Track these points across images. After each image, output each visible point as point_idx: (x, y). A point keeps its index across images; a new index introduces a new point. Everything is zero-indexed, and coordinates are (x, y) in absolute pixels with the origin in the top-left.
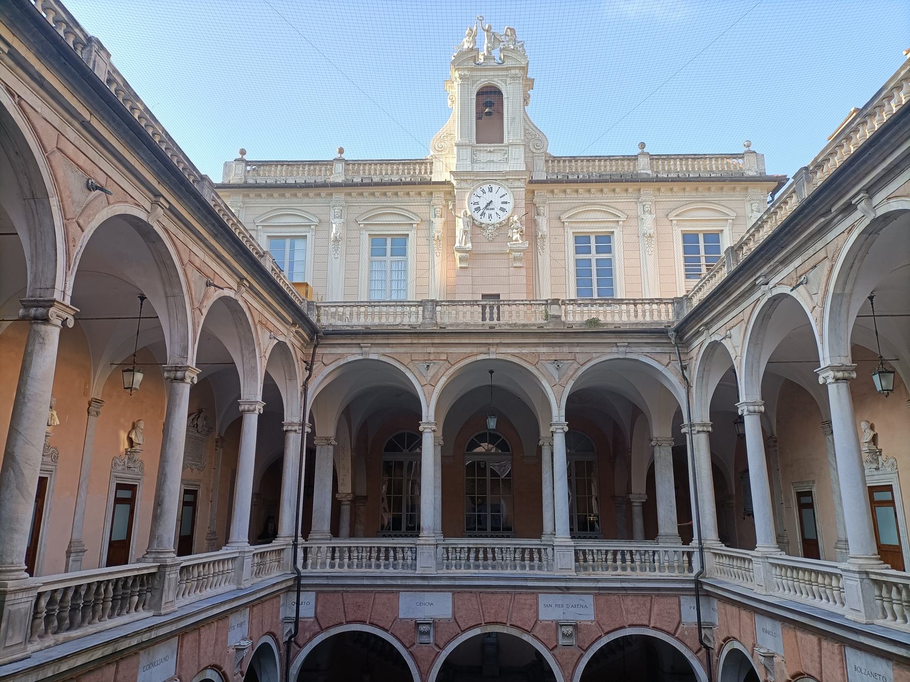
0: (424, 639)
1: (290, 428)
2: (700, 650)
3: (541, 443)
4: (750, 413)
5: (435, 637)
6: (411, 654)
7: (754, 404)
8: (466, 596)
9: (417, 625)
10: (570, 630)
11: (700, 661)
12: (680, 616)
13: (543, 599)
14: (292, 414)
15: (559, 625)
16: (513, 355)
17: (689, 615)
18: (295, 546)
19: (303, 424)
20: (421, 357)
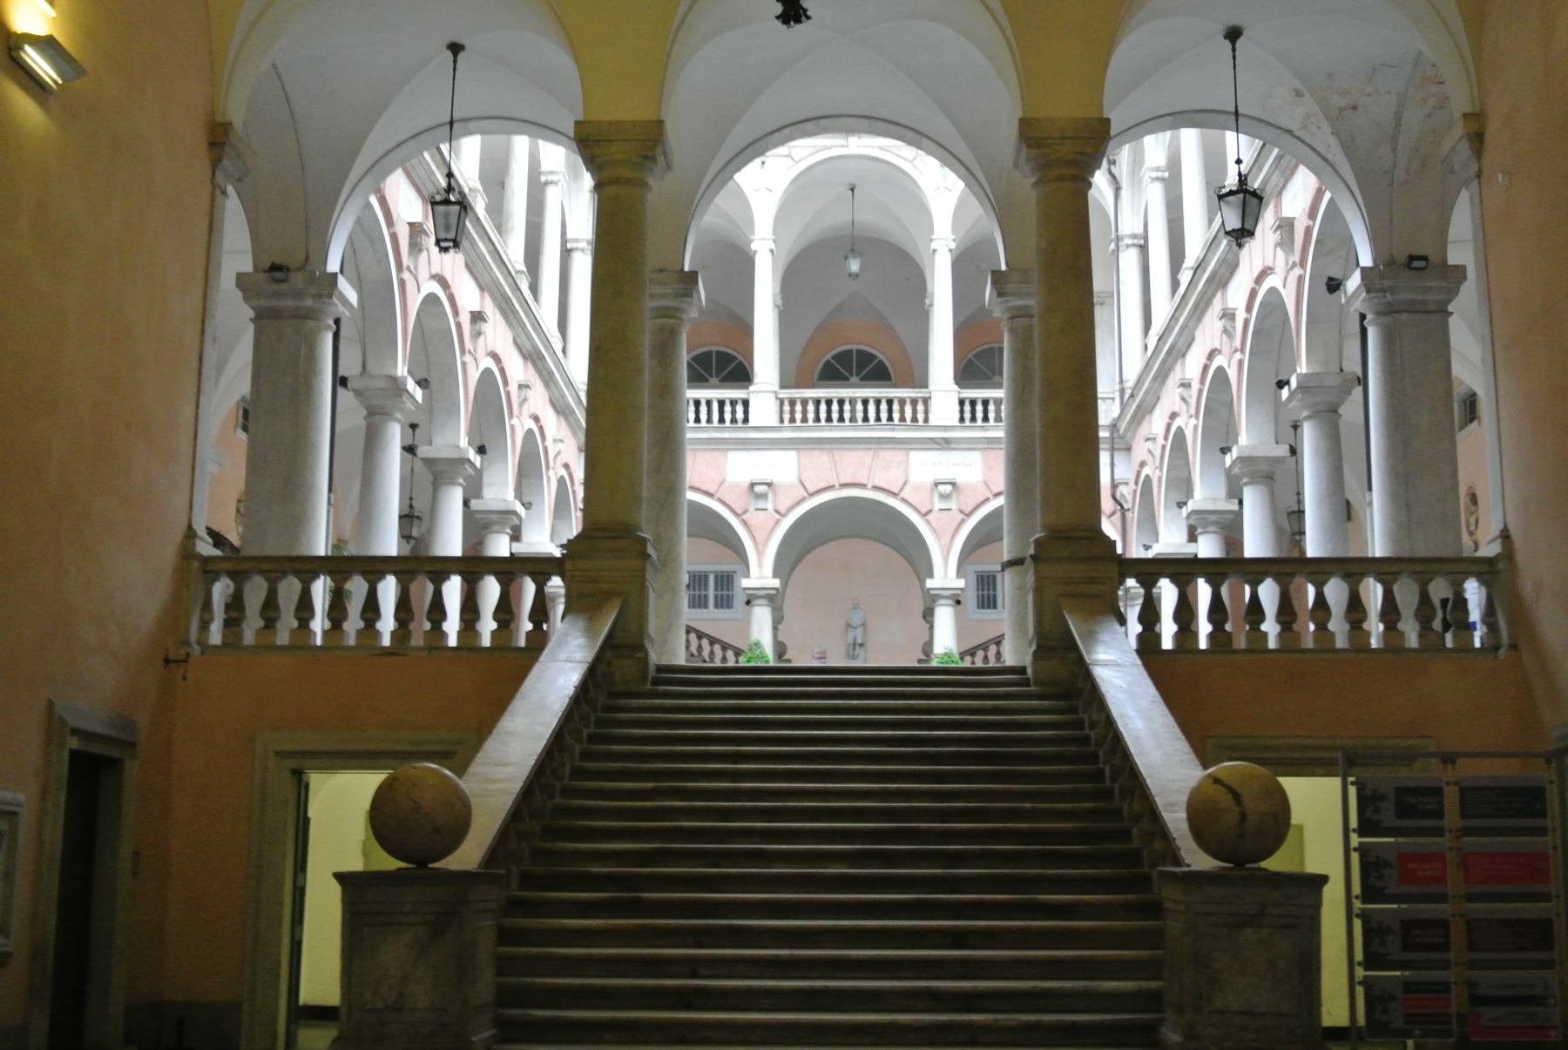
0: (761, 505)
2: (1114, 513)
3: (927, 302)
5: (775, 503)
6: (744, 523)
7: (1158, 169)
8: (816, 453)
9: (752, 485)
10: (949, 488)
11: (1114, 525)
13: (916, 456)
15: (936, 484)
16: (881, 148)
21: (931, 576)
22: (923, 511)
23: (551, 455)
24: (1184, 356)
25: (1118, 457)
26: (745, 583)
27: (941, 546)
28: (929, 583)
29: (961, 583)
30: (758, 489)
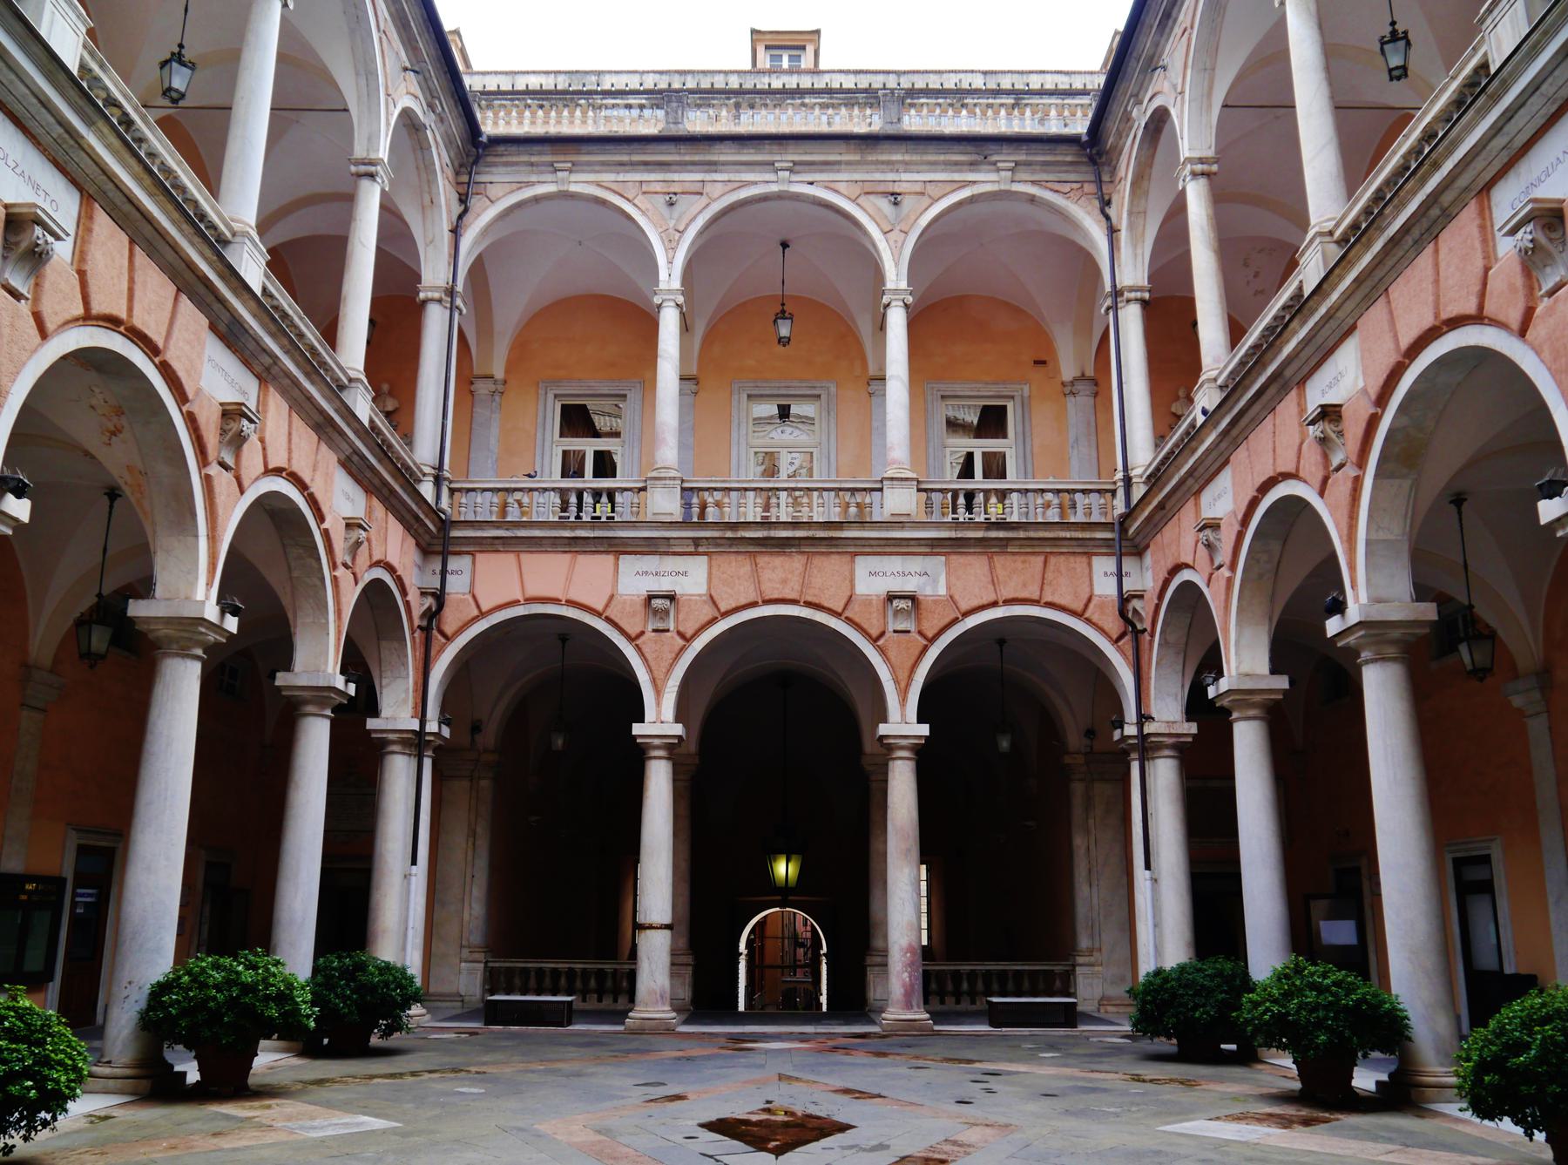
1: (430, 295)
4: (1194, 175)
7: (1201, 161)
9: (650, 597)
12: (1091, 585)
13: (863, 565)
14: (434, 273)
15: (891, 597)
17: (1105, 587)
18: (438, 480)
19: (451, 292)
20: (658, 187)
21: (885, 721)
22: (874, 632)
23: (340, 546)
24: (1302, 383)
25: (1129, 564)
26: (637, 729)
27: (896, 682)
28: (883, 729)
29: (925, 730)
30: (657, 603)
